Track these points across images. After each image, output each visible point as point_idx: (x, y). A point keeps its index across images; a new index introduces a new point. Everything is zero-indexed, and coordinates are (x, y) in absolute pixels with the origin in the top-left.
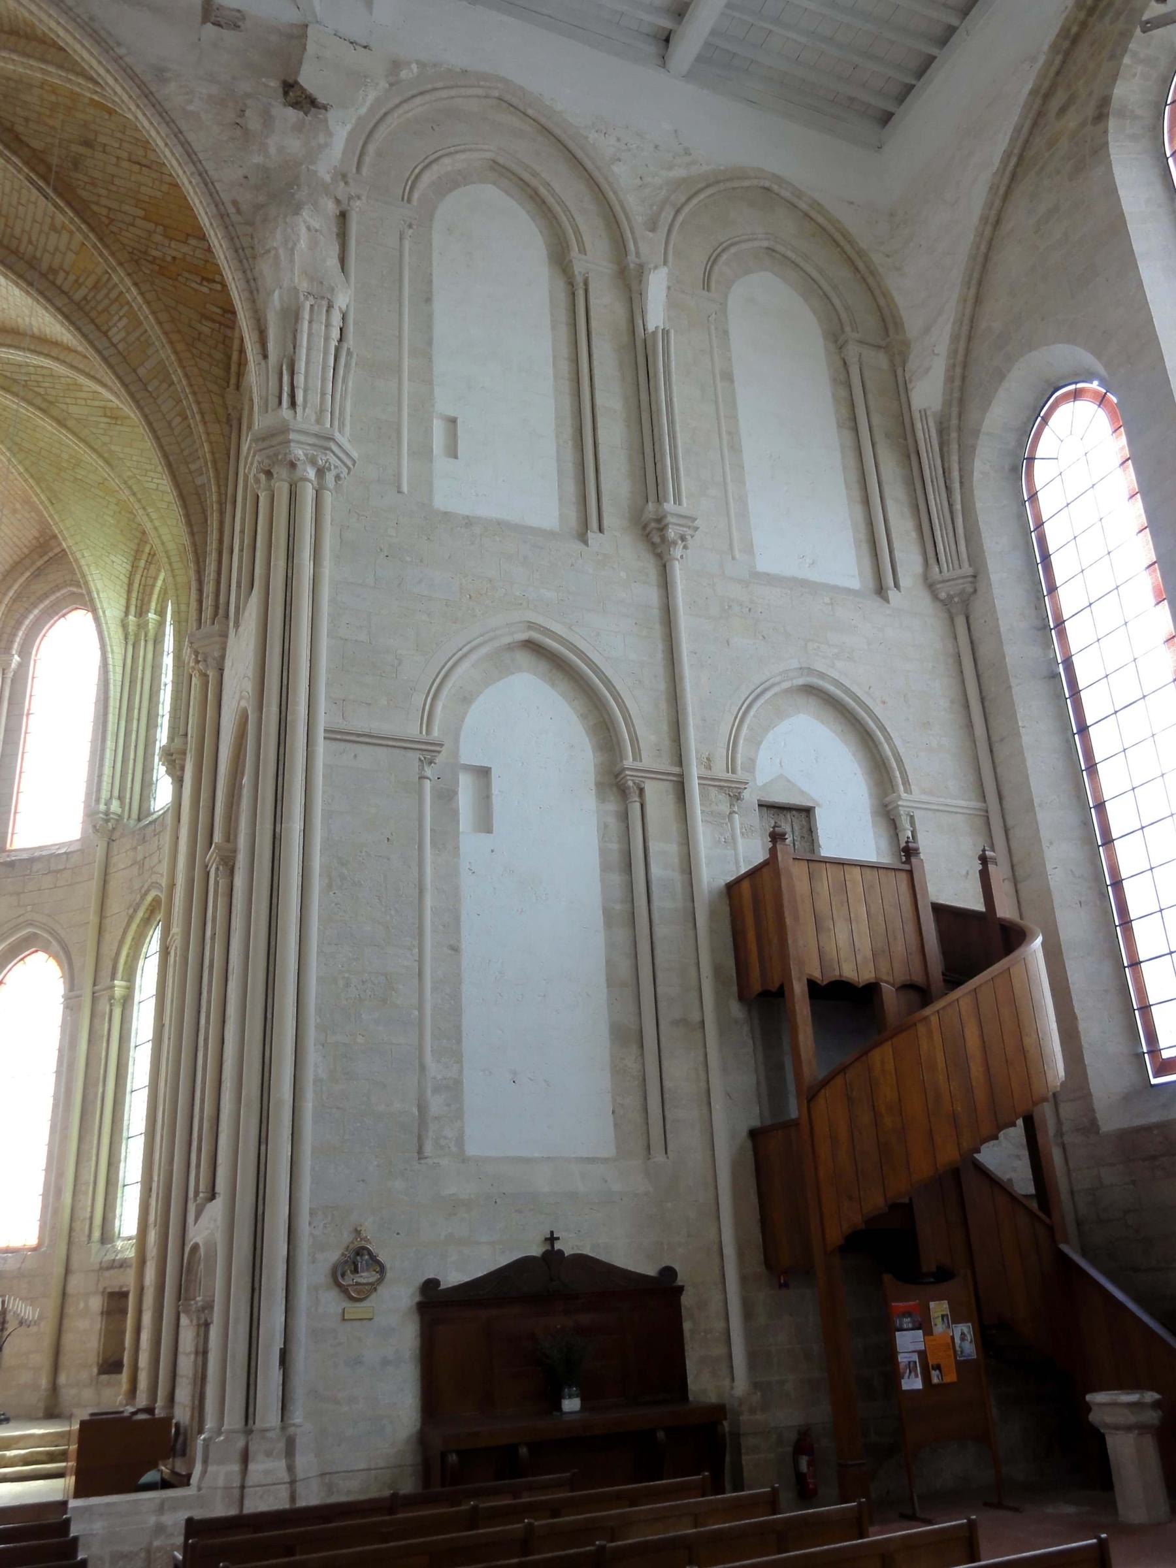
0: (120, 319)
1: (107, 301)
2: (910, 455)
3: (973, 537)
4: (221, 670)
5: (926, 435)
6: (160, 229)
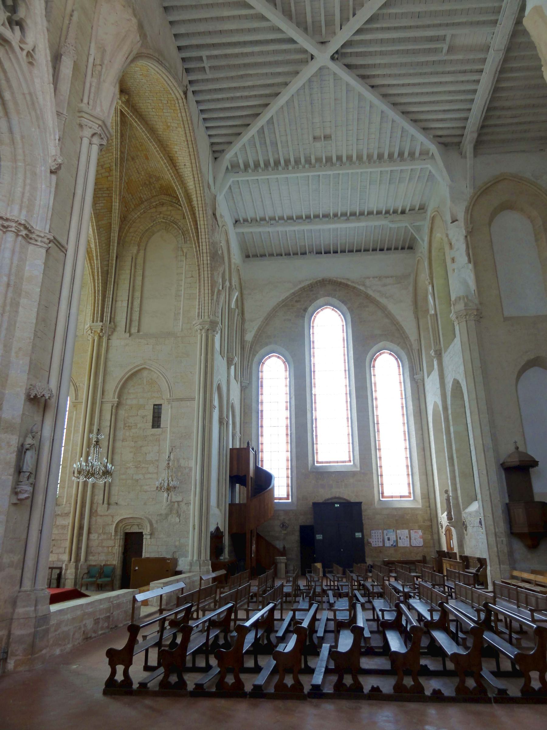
0: (102, 203)
1: (101, 195)
2: (243, 348)
3: (251, 373)
4: (109, 339)
5: (248, 346)
6: (127, 188)
